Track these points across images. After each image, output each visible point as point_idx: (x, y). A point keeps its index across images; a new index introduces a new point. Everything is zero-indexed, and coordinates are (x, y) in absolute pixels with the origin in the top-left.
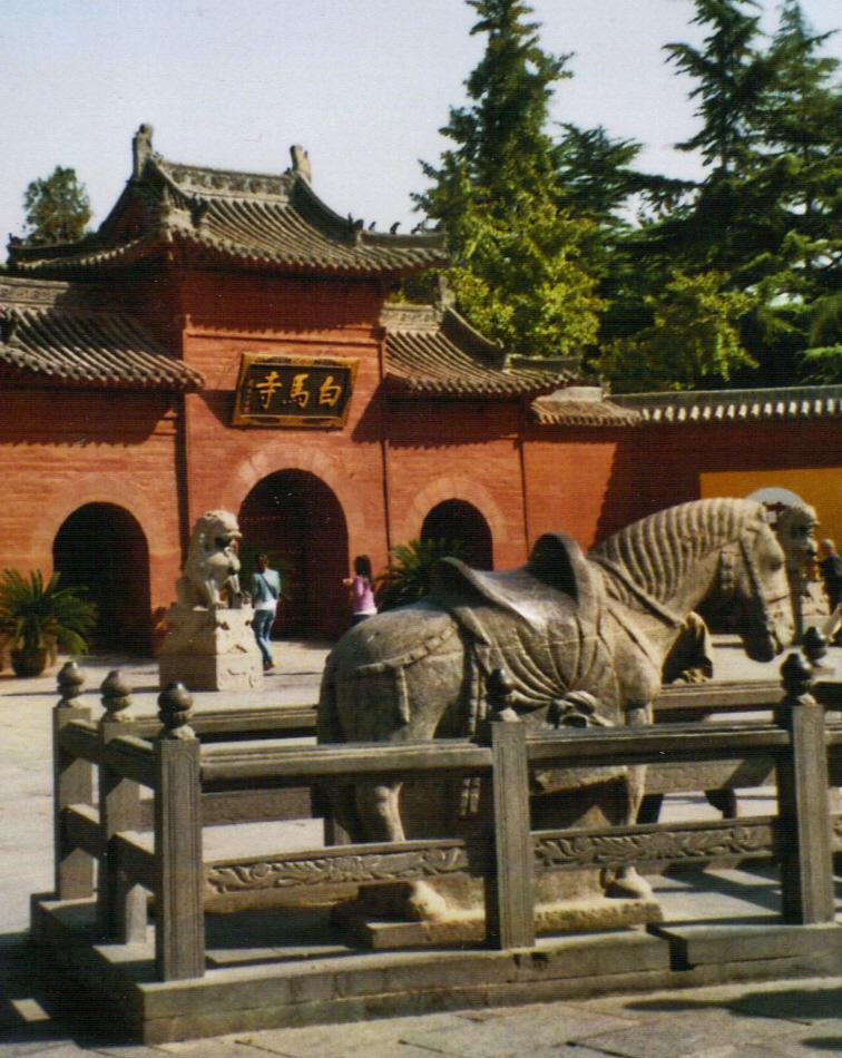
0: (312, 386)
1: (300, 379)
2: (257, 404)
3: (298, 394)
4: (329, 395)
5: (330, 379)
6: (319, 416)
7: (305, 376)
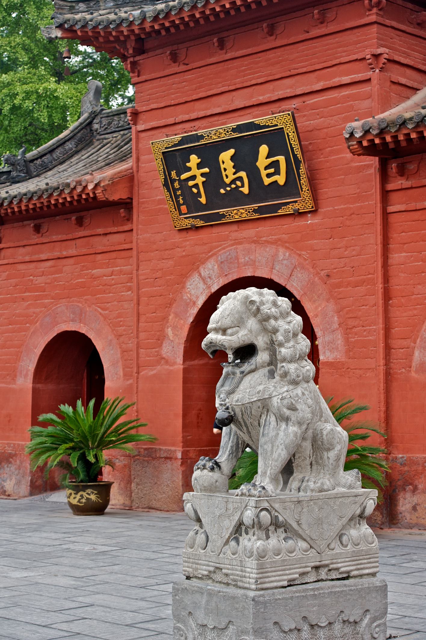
0: (245, 161)
3: (232, 177)
4: (272, 170)
5: (264, 149)
6: (268, 201)
7: (232, 151)
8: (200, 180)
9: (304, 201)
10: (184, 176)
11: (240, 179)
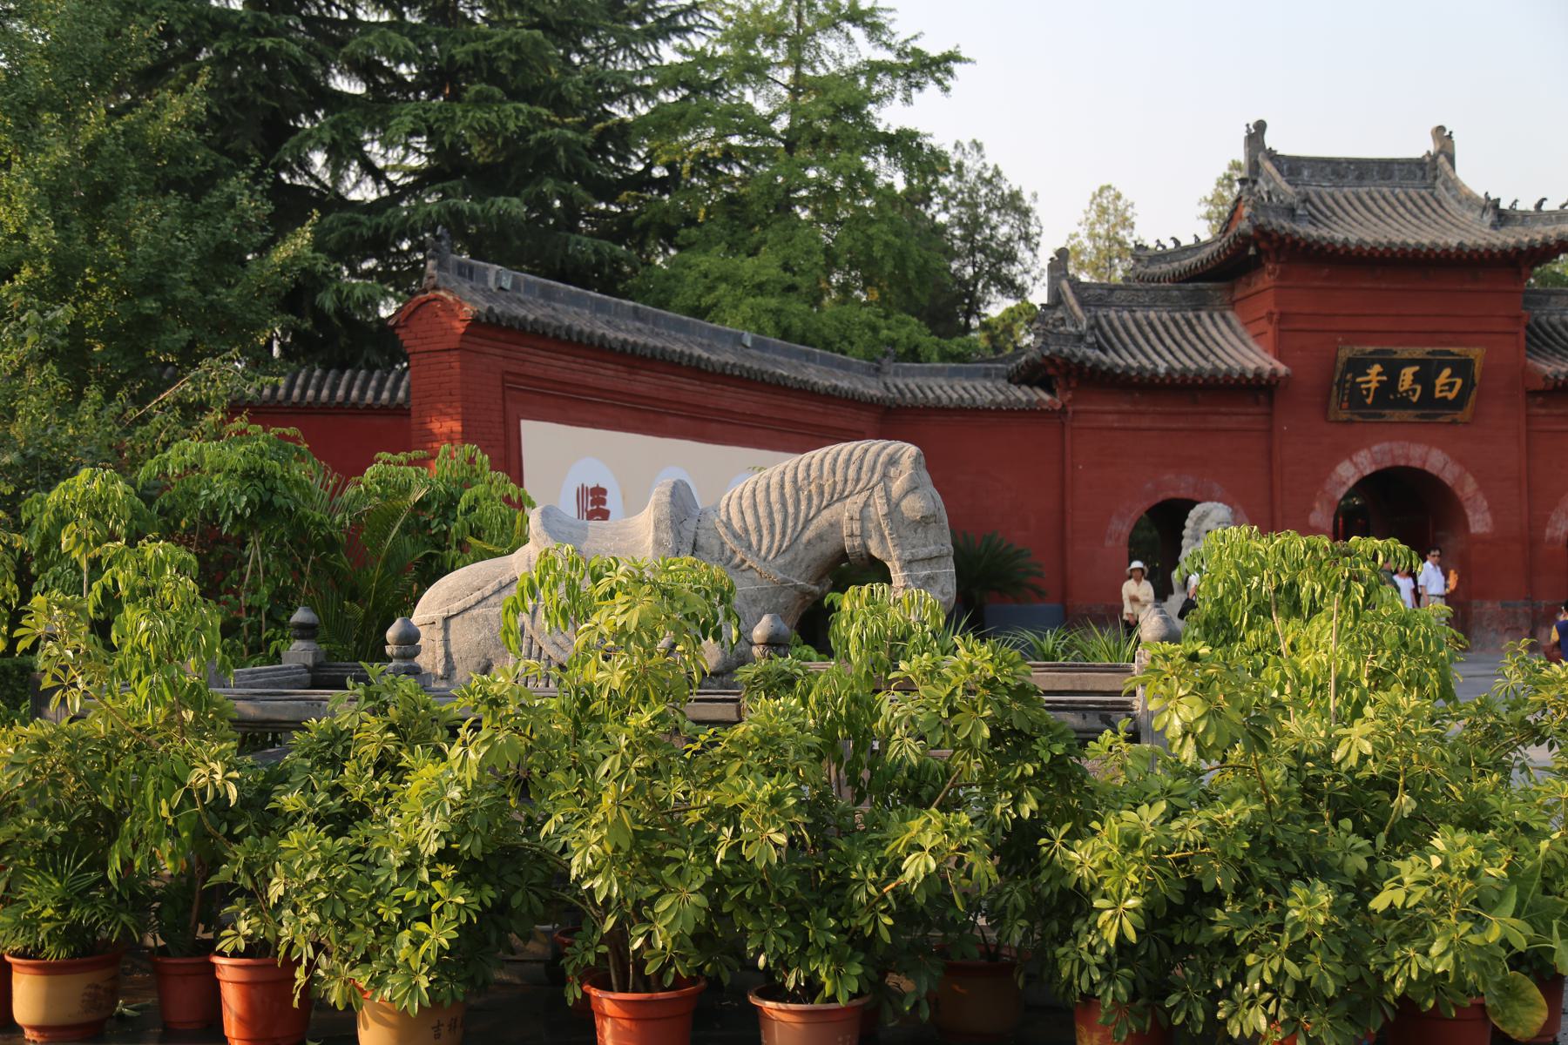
0: (1426, 377)
1: (1408, 374)
2: (1355, 397)
5: (1447, 372)
8: (1373, 385)
9: (1464, 415)
10: (1359, 380)
11: (1414, 391)
